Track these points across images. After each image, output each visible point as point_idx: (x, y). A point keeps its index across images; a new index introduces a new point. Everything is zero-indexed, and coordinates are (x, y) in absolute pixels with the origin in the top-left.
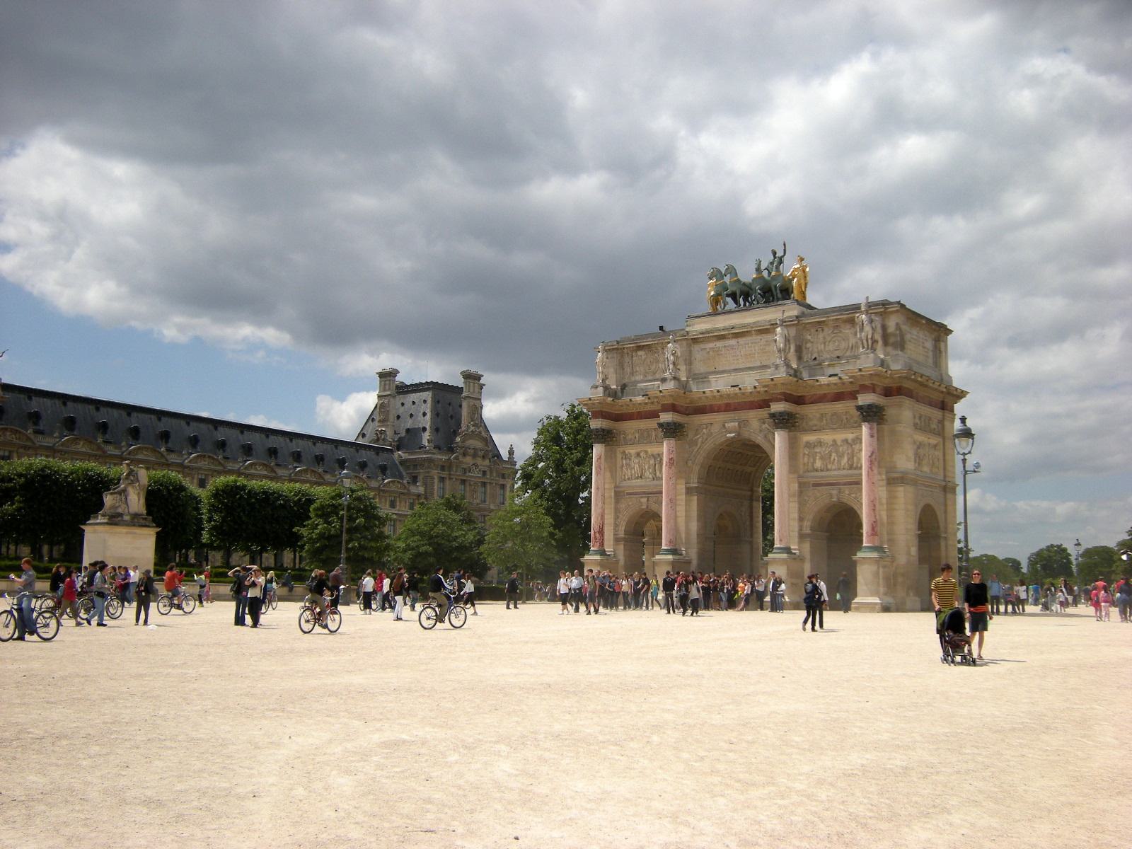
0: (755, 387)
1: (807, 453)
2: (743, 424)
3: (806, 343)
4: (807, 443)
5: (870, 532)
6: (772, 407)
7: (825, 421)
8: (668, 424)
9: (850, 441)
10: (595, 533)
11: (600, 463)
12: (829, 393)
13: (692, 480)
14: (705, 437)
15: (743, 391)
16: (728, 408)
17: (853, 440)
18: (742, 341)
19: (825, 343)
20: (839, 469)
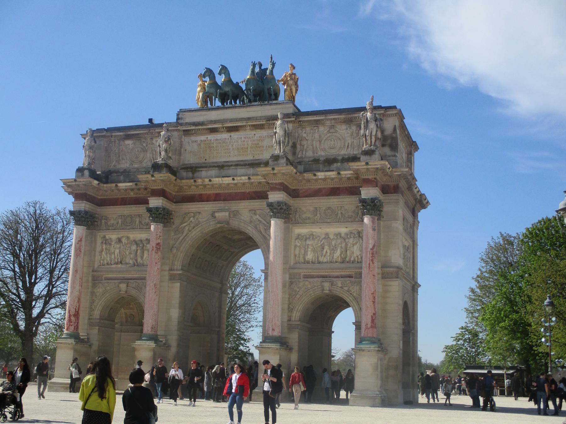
0: (249, 178)
1: (299, 245)
2: (235, 214)
3: (301, 140)
4: (299, 235)
5: (369, 326)
6: (269, 197)
7: (318, 215)
8: (157, 209)
9: (343, 235)
10: (70, 316)
11: (80, 246)
12: (324, 188)
13: (175, 267)
14: (192, 225)
15: (235, 182)
16: (217, 198)
17: (347, 234)
18: (235, 135)
19: (320, 142)
20: (331, 262)
